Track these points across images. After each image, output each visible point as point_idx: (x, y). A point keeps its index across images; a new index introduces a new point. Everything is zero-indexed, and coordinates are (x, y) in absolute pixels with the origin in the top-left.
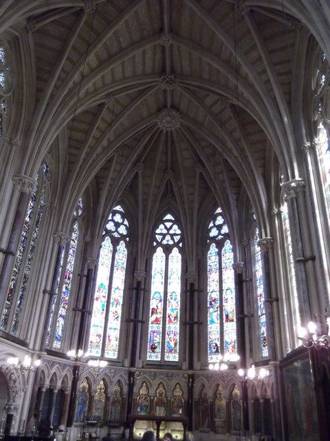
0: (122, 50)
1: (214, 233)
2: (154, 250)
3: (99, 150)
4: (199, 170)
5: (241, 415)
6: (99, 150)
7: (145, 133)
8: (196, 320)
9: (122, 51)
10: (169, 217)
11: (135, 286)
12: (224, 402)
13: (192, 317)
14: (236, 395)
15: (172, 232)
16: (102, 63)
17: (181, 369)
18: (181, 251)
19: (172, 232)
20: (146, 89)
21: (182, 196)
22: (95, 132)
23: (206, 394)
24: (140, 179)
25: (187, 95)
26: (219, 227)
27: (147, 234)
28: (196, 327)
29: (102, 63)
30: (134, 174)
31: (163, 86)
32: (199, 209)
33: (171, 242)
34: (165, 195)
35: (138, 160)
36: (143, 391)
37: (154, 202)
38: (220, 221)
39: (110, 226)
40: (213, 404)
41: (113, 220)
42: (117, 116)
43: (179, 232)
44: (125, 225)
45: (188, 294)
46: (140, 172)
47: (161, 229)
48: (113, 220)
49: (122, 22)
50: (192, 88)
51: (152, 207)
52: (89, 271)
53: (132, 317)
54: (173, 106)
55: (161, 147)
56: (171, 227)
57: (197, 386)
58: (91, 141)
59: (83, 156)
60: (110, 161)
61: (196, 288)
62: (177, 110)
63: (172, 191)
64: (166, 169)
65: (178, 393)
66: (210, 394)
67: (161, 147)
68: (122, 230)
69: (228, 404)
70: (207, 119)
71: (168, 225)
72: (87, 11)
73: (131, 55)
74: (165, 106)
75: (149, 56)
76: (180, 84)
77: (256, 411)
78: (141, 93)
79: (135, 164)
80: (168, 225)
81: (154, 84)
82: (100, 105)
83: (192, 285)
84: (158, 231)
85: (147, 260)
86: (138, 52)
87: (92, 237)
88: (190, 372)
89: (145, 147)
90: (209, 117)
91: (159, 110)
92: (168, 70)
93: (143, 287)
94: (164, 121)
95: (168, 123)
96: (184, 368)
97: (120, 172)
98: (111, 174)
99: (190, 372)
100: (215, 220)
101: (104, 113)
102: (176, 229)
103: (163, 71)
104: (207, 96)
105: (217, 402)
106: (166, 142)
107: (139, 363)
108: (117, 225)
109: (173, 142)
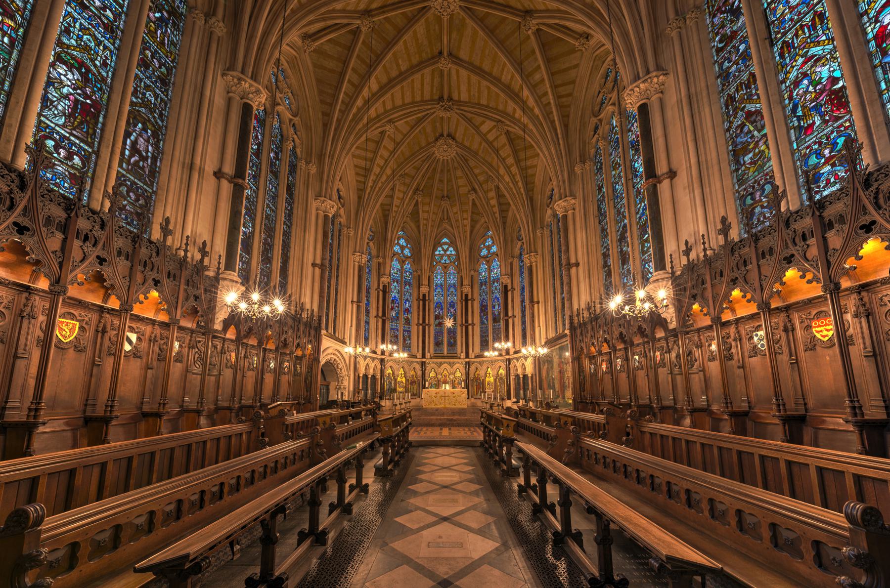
0: (401, 74)
1: (484, 252)
2: (432, 268)
3: (384, 178)
4: (472, 196)
5: (505, 386)
6: (384, 178)
7: (423, 162)
8: (470, 322)
9: (402, 76)
10: (445, 240)
11: (421, 298)
12: (492, 379)
13: (467, 321)
14: (501, 374)
15: (448, 253)
16: (384, 88)
17: (460, 358)
18: (459, 268)
19: (448, 253)
20: (424, 116)
21: (457, 221)
22: (380, 161)
23: (478, 375)
24: (420, 206)
25: (463, 122)
26: (489, 248)
27: (429, 255)
28: (470, 327)
29: (384, 88)
30: (414, 202)
31: (442, 114)
32: (471, 232)
33: (448, 262)
34: (442, 220)
35: (417, 189)
36: (432, 374)
37: (432, 226)
38: (489, 242)
39: (397, 249)
40: (484, 380)
41: (398, 244)
42: (398, 144)
43: (453, 253)
44: (408, 248)
45: (464, 302)
46: (420, 200)
47: (439, 251)
48: (398, 244)
49: (401, 43)
50: (469, 115)
51: (431, 231)
52: (384, 286)
53: (421, 322)
54: (449, 135)
55: (438, 175)
56: (447, 250)
57: (472, 368)
58: (376, 170)
59: (370, 184)
60: (393, 189)
61: (470, 297)
62: (454, 139)
63: (449, 218)
64: (443, 197)
65: (458, 374)
66: (482, 373)
67: (438, 175)
68: (407, 252)
69: (495, 380)
70: (482, 147)
71: (445, 247)
72: (364, 29)
73: (410, 80)
74: (442, 135)
75: (428, 79)
76: (458, 111)
77: (517, 383)
78: (420, 121)
79: (414, 193)
80: (445, 247)
81: (432, 111)
82: (381, 133)
83: (466, 295)
84: (437, 253)
85: (429, 277)
86: (417, 76)
87: (384, 258)
88: (467, 360)
89: (423, 176)
90: (484, 144)
91: (437, 140)
92: (445, 97)
93: (427, 298)
94: (441, 149)
95: (444, 152)
96: (462, 357)
97: (403, 199)
98: (396, 202)
99: (467, 360)
100: (485, 241)
101: (386, 142)
102: (451, 251)
103: (441, 98)
104: (484, 122)
105: (487, 379)
106: (442, 171)
107: (428, 355)
108: (402, 248)
109: (449, 171)
